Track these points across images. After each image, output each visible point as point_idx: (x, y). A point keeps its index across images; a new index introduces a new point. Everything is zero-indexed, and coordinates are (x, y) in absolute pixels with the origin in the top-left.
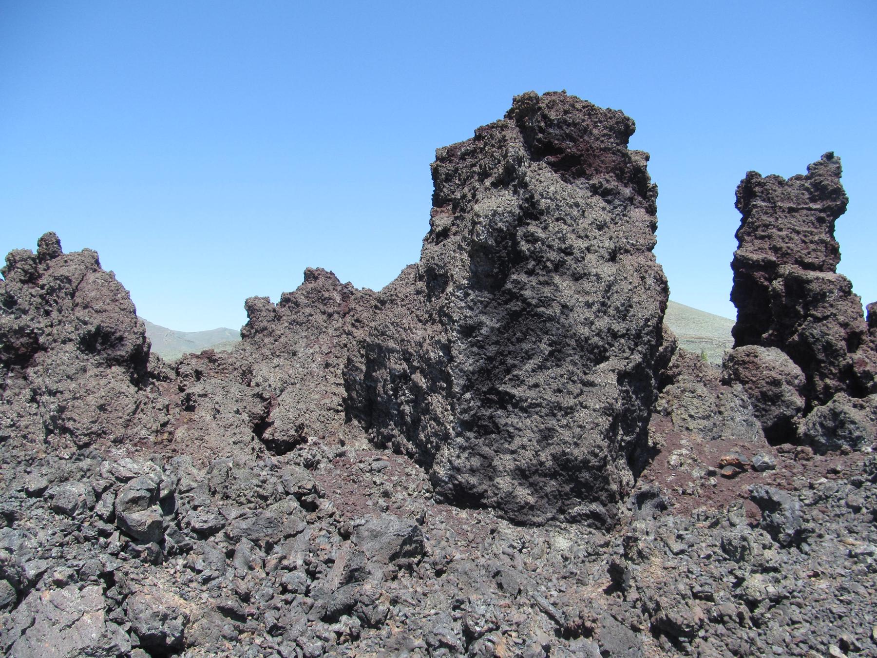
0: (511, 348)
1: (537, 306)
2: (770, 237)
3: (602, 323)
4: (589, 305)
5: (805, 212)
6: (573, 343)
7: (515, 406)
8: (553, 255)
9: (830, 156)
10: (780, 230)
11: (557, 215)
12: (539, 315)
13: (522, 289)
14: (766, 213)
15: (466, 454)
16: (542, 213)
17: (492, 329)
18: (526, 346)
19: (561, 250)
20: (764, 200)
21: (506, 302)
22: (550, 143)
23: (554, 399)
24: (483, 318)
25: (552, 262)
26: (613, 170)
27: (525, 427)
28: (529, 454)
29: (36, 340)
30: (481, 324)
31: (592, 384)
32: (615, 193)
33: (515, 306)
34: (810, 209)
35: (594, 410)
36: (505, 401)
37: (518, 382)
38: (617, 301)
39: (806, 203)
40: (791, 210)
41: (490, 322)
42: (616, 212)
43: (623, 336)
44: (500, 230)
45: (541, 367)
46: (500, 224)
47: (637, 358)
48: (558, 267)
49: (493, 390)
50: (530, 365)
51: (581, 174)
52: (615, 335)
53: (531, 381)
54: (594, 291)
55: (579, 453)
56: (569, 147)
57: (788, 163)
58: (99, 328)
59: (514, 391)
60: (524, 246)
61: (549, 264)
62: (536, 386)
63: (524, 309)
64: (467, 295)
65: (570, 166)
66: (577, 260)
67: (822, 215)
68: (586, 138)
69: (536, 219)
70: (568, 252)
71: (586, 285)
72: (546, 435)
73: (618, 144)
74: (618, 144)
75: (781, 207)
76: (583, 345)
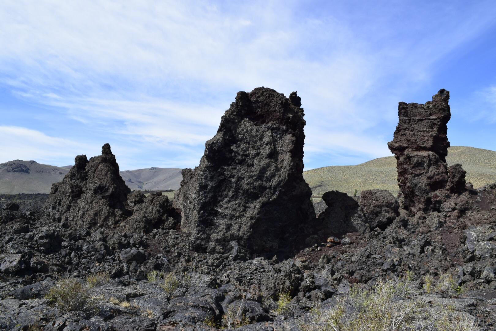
0: (220, 194)
1: (230, 177)
2: (406, 135)
3: (257, 184)
4: (251, 177)
5: (426, 121)
6: (242, 192)
7: (220, 215)
8: (240, 157)
9: (442, 91)
10: (412, 131)
11: (245, 141)
12: (231, 181)
13: (225, 171)
14: (405, 123)
15: (201, 233)
16: (238, 141)
17: (212, 187)
18: (225, 193)
19: (243, 155)
20: (405, 117)
21: (218, 176)
23: (233, 213)
24: (209, 183)
26: (278, 119)
27: (222, 223)
28: (221, 234)
29: (81, 189)
30: (209, 184)
31: (249, 207)
32: (278, 129)
33: (222, 177)
34: (429, 119)
35: (248, 217)
36: (216, 214)
37: (221, 207)
38: (268, 174)
39: (427, 116)
40: (419, 120)
41: (211, 184)
42: (279, 136)
43: (269, 188)
44: (215, 149)
45: (229, 201)
46: (215, 147)
47: (275, 197)
48: (242, 162)
49: (213, 209)
50: (226, 199)
52: (265, 188)
53: (225, 206)
54: (256, 170)
55: (241, 233)
57: (422, 96)
58: (100, 185)
59: (219, 210)
60: (228, 155)
61: (237, 161)
62: (227, 208)
63: (225, 179)
64: (204, 174)
65: (258, 119)
66: (251, 159)
68: (266, 107)
69: (236, 143)
70: (248, 156)
71: (253, 169)
72: (229, 227)
73: (280, 108)
74: (280, 108)
75: (413, 119)
76: (246, 192)
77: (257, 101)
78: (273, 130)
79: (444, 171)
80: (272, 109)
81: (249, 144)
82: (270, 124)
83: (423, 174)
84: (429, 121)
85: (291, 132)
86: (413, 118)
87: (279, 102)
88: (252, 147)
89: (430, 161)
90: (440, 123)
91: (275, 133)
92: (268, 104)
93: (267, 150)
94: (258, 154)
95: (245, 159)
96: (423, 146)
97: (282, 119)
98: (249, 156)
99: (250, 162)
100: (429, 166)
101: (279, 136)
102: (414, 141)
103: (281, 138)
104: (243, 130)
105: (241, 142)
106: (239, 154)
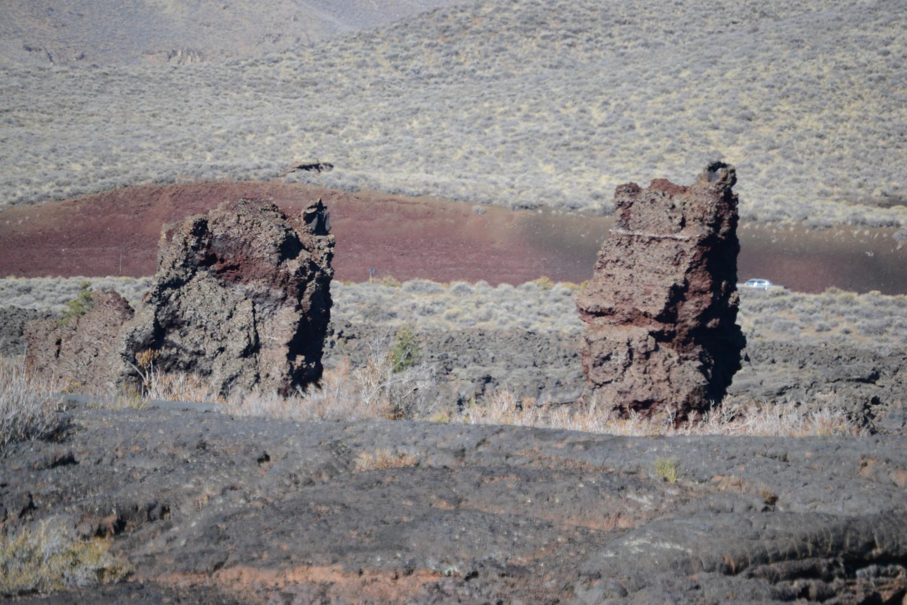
8: (186, 358)
9: (714, 167)
10: (629, 267)
11: (199, 323)
19: (193, 353)
22: (214, 255)
25: (184, 363)
34: (676, 240)
42: (267, 310)
44: (138, 343)
48: (189, 367)
51: (237, 279)
56: (230, 260)
66: (207, 360)
67: (687, 248)
75: (639, 236)
77: (226, 237)
78: (256, 298)
79: (664, 377)
80: (256, 255)
81: (205, 329)
82: (250, 286)
83: (609, 382)
84: (674, 243)
85: (292, 302)
86: (637, 233)
87: (271, 241)
88: (212, 336)
89: (631, 352)
90: (694, 252)
91: (261, 303)
92: (246, 244)
93: (238, 344)
94: (222, 350)
95: (196, 361)
96: (643, 310)
97: (275, 276)
98: (204, 354)
99: (205, 366)
100: (626, 366)
101: (267, 310)
102: (627, 297)
103: (272, 314)
104: (194, 300)
105: (189, 324)
106: (185, 351)
